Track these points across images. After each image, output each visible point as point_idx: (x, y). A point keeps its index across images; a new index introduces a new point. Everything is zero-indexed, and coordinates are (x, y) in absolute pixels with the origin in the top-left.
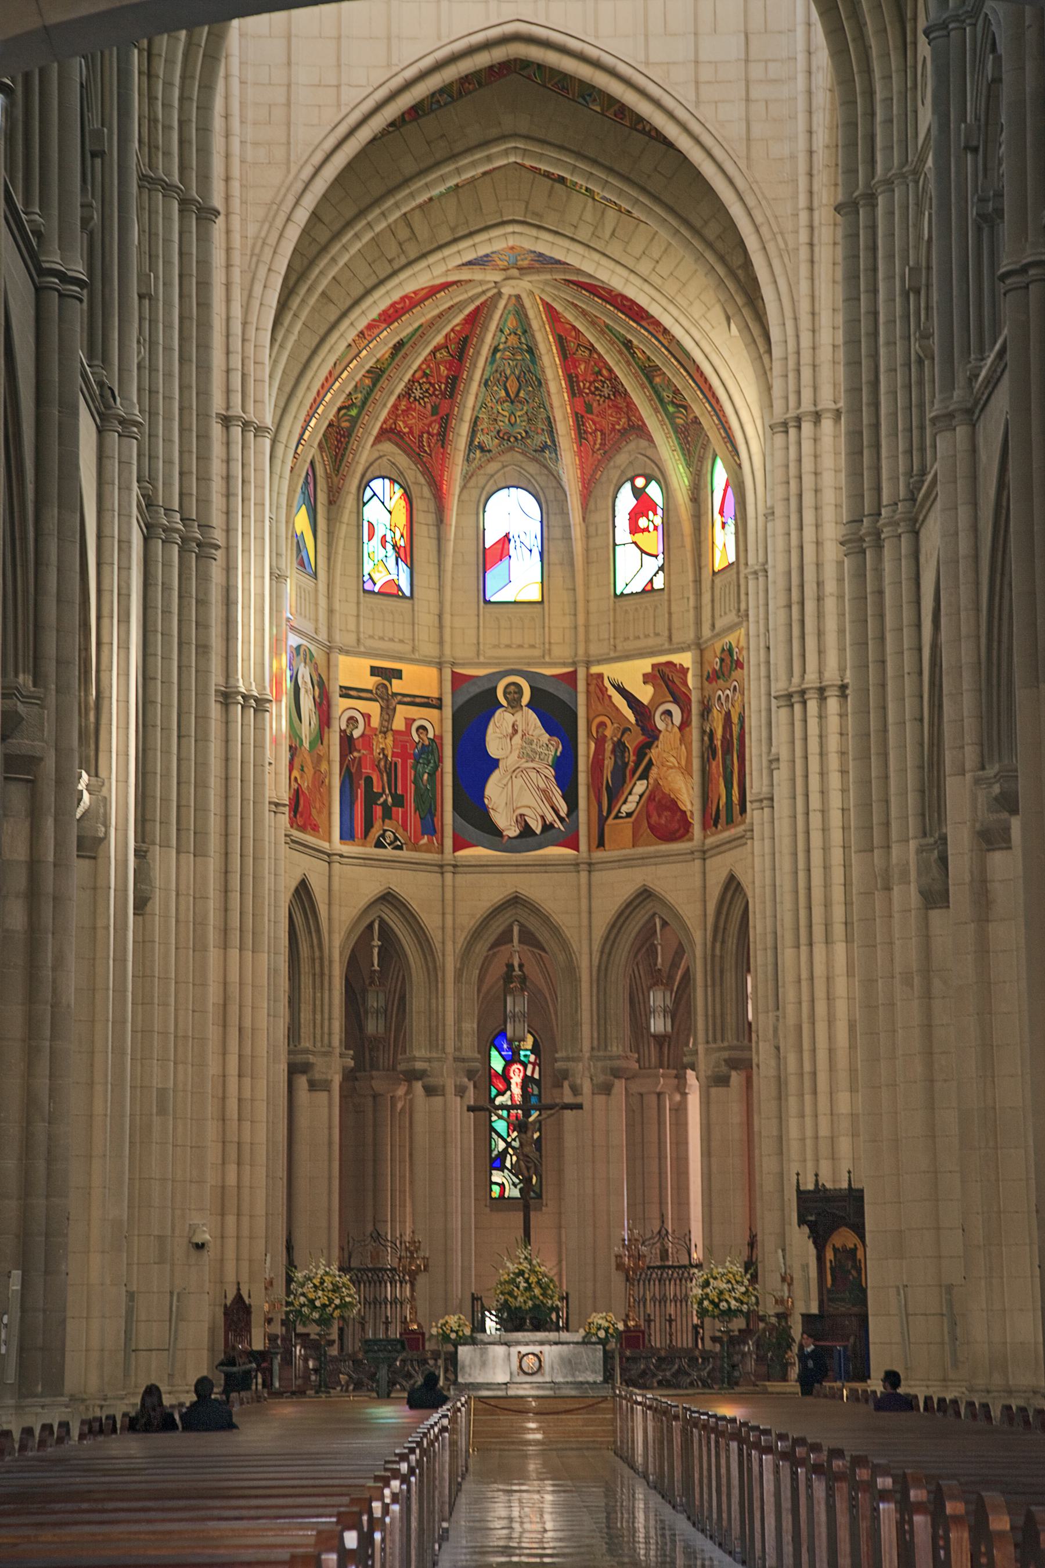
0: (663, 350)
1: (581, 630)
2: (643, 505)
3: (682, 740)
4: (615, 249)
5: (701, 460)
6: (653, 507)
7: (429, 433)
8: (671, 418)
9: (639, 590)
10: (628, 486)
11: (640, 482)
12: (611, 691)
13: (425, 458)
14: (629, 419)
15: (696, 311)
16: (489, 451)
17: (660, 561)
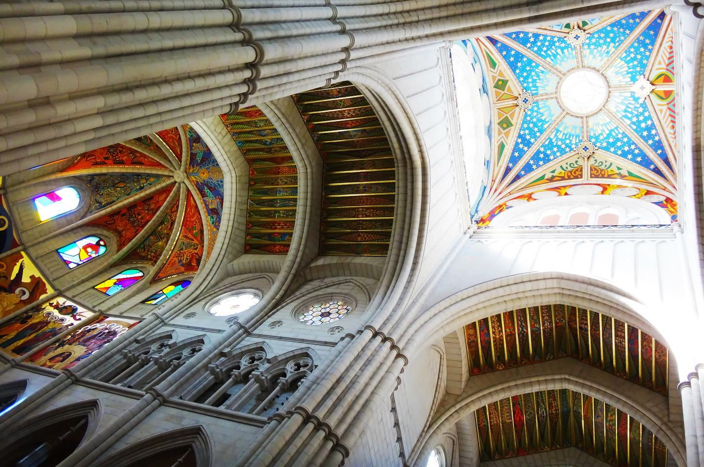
0: (177, 238)
1: (37, 241)
2: (96, 247)
3: (16, 304)
4: (238, 212)
5: (125, 264)
6: (97, 252)
7: (95, 158)
8: (139, 247)
9: (65, 259)
10: (97, 239)
11: (102, 243)
12: (18, 264)
13: (84, 159)
14: (122, 231)
15: (229, 250)
16: (91, 183)
17: (81, 263)
